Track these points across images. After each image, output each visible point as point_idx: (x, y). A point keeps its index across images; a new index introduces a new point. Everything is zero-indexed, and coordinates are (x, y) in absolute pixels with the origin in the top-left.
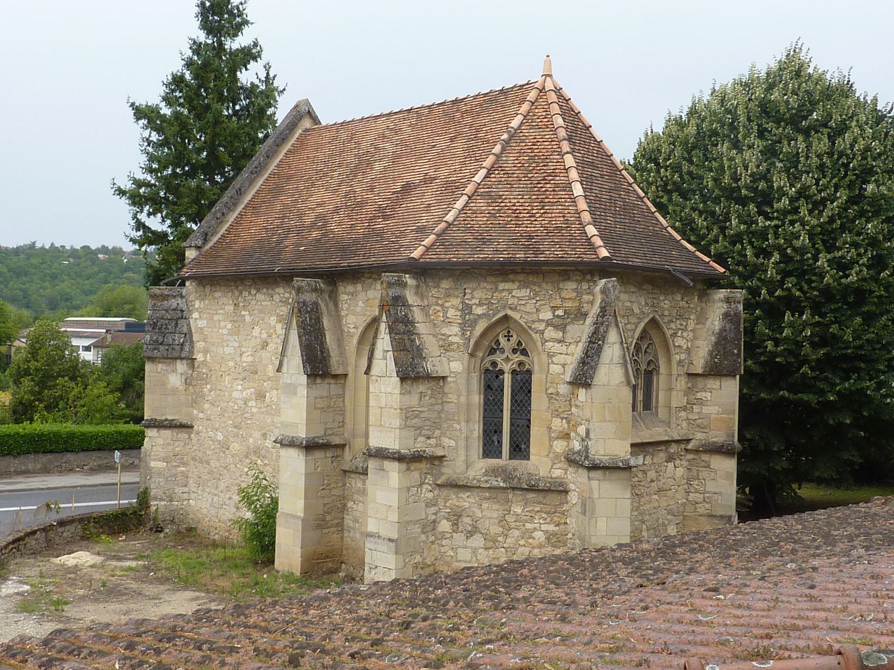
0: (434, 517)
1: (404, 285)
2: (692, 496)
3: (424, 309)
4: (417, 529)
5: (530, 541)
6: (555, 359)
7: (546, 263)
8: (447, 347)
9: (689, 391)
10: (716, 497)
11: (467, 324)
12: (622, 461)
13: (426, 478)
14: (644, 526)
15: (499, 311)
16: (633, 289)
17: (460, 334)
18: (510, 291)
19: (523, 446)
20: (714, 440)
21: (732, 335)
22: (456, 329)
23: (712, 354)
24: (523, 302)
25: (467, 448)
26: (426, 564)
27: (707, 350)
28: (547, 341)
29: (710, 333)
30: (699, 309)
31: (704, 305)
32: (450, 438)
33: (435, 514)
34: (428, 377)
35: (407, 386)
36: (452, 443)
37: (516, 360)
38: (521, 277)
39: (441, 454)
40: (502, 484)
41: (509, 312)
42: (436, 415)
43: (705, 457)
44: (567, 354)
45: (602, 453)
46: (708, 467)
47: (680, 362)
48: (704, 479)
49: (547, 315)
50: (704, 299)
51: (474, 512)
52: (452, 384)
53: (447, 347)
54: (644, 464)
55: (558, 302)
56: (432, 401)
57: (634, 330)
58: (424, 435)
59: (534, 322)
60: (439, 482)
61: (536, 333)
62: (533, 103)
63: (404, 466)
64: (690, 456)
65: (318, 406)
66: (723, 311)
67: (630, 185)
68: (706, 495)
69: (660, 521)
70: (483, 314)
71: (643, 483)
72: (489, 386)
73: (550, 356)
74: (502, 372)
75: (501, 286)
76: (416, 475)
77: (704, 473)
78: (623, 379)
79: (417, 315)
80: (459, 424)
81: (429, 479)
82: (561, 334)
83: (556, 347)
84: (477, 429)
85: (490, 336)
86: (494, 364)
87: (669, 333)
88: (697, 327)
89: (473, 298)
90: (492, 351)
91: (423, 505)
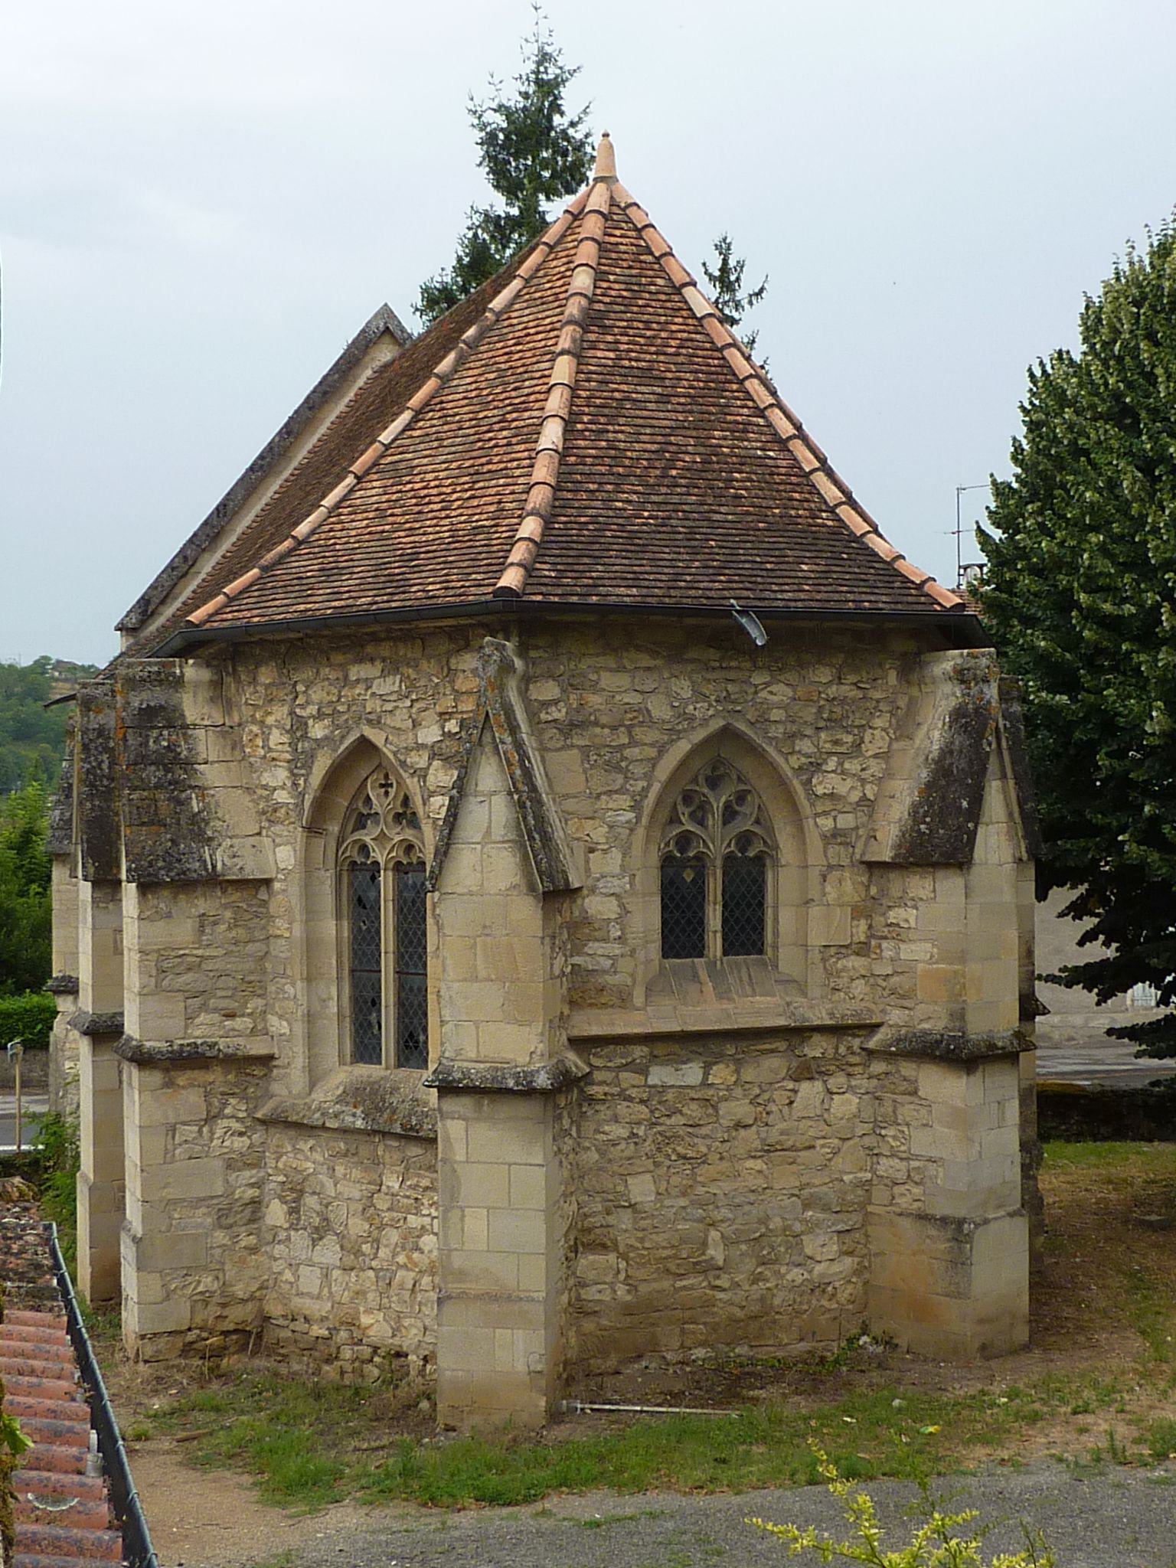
0: (251, 1192)
1: (179, 682)
2: (886, 1166)
3: (228, 733)
4: (203, 1218)
5: (416, 1255)
7: (420, 613)
8: (270, 814)
10: (932, 1167)
11: (300, 763)
12: (517, 1076)
13: (225, 1105)
14: (714, 1235)
15: (349, 730)
16: (646, 661)
17: (289, 784)
18: (368, 683)
20: (926, 1026)
21: (963, 765)
22: (282, 775)
23: (916, 812)
24: (389, 707)
25: (312, 1040)
26: (233, 1296)
27: (908, 801)
29: (922, 759)
30: (902, 702)
31: (914, 691)
32: (281, 1017)
33: (257, 1185)
34: (214, 881)
35: (162, 901)
37: (397, 839)
38: (385, 650)
39: (262, 1050)
40: (359, 1124)
41: (370, 733)
42: (250, 965)
43: (908, 1069)
45: (473, 1055)
46: (914, 1093)
47: (835, 836)
48: (908, 1125)
49: (430, 734)
50: (915, 677)
51: (323, 1185)
52: (280, 897)
53: (270, 814)
54: (705, 1084)
55: (447, 703)
56: (240, 933)
57: (654, 762)
58: (215, 1010)
60: (259, 1115)
62: (551, 247)
63: (156, 1077)
64: (878, 1067)
66: (953, 703)
67: (761, 413)
68: (914, 1164)
69: (776, 1223)
70: (326, 738)
71: (704, 1131)
72: (360, 900)
75: (356, 672)
76: (193, 1098)
77: (906, 1112)
78: (517, 879)
79: (206, 745)
80: (293, 985)
81: (235, 1106)
84: (335, 997)
85: (350, 786)
86: (364, 849)
87: (787, 766)
88: (895, 746)
89: (308, 703)
90: (361, 823)
91: (219, 1164)
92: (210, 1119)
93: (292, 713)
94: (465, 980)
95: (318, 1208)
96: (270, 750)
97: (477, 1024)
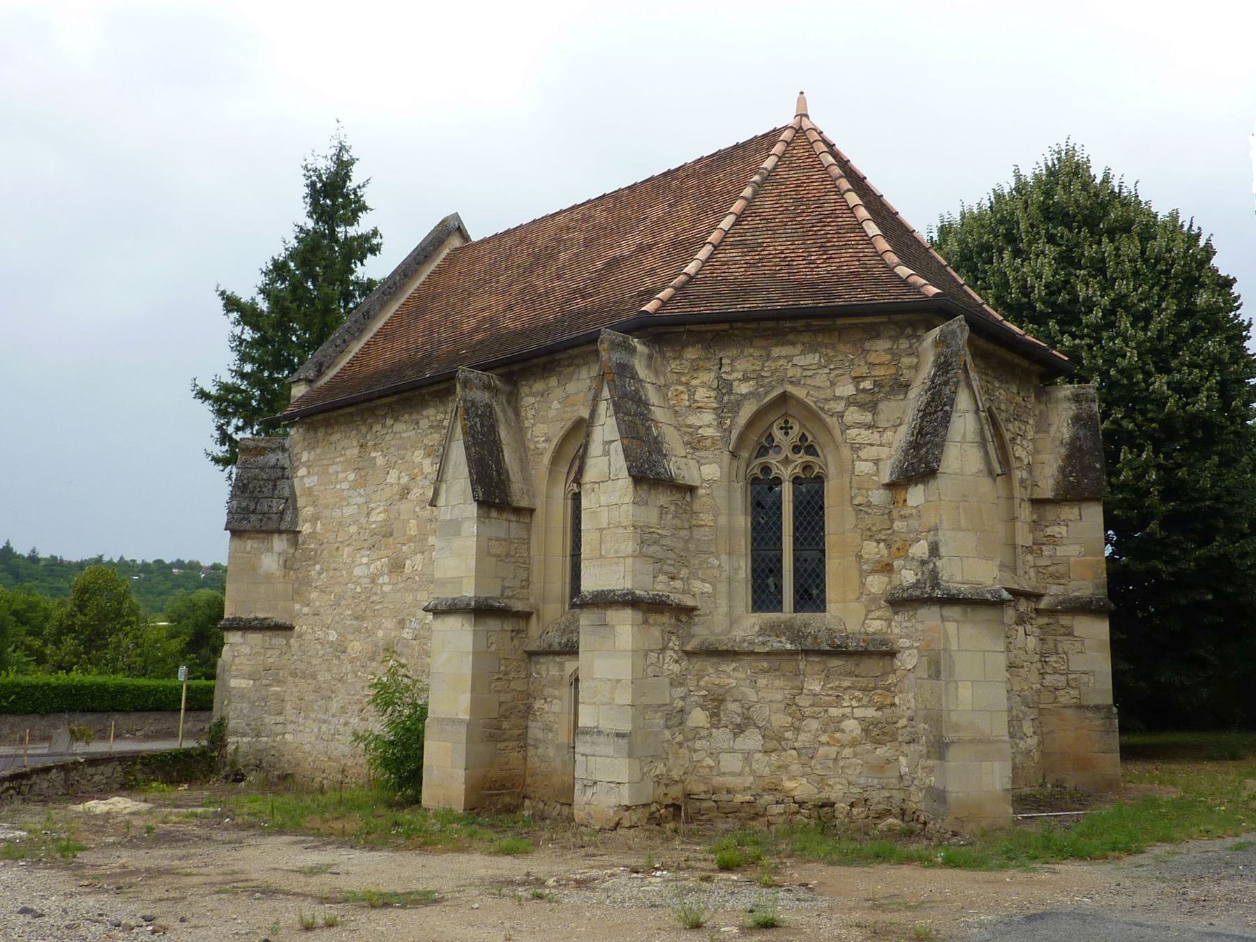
0: (681, 703)
1: (633, 351)
2: (1049, 679)
4: (659, 720)
5: (838, 735)
6: (862, 454)
8: (695, 444)
9: (1036, 525)
10: (1085, 678)
11: (726, 406)
12: (989, 591)
15: (773, 388)
17: (715, 423)
18: (789, 358)
19: (815, 592)
20: (1077, 594)
21: (1089, 444)
22: (708, 417)
24: (810, 373)
25: (730, 595)
26: (671, 779)
27: (1055, 466)
28: (848, 427)
30: (1037, 412)
31: (1043, 407)
32: (703, 581)
33: (683, 698)
35: (643, 492)
36: (708, 588)
37: (800, 461)
38: (806, 338)
40: (789, 646)
41: (790, 389)
43: (1065, 620)
44: (880, 445)
45: (959, 579)
46: (1070, 634)
48: (1066, 653)
49: (847, 390)
51: (744, 694)
53: (695, 444)
55: (864, 370)
58: (666, 573)
59: (827, 400)
60: (688, 648)
61: (832, 416)
62: (788, 144)
63: (639, 616)
64: (1043, 621)
65: (493, 551)
68: (1071, 676)
70: (750, 393)
73: (856, 448)
74: (778, 481)
75: (776, 351)
76: (656, 632)
77: (1065, 644)
78: (982, 467)
79: (652, 396)
81: (674, 643)
82: (870, 416)
83: (864, 435)
84: (743, 569)
86: (766, 469)
87: (1008, 436)
89: (733, 371)
90: (763, 451)
91: (667, 681)
92: (664, 649)
93: (719, 378)
94: (953, 529)
95: (739, 711)
96: (696, 401)
97: (961, 558)
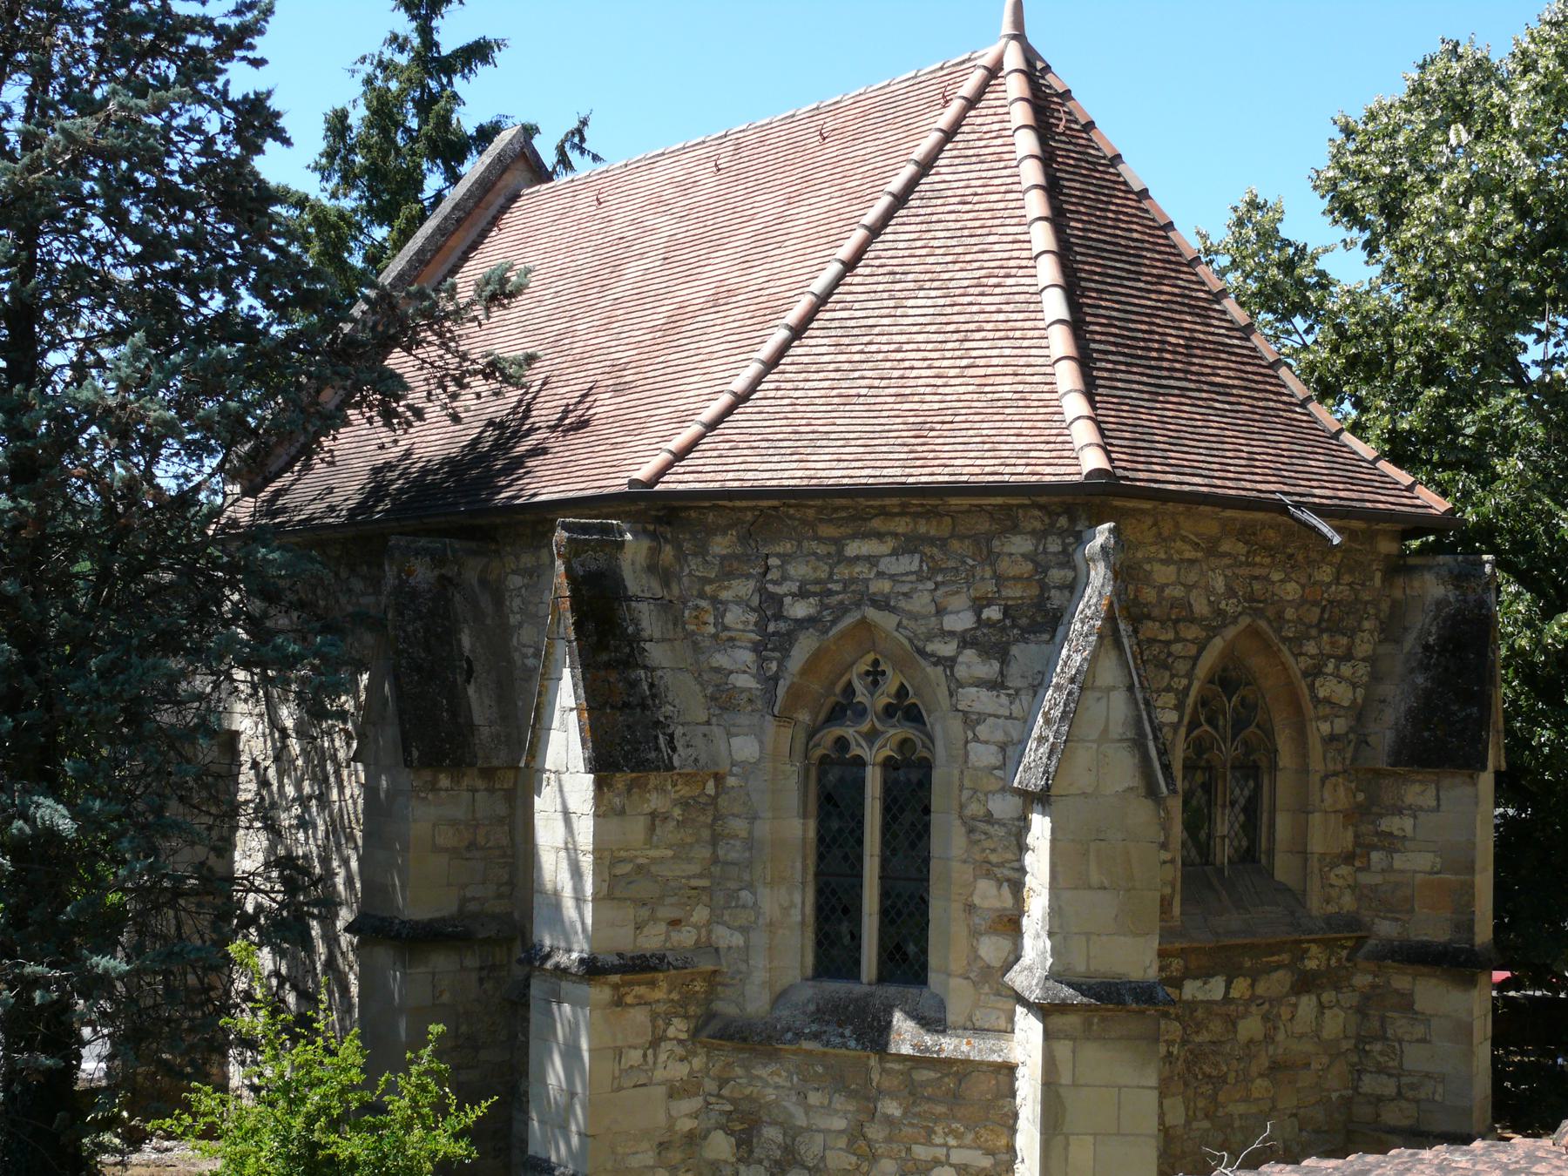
6: (982, 730)
9: (1361, 814)
11: (773, 641)
19: (911, 949)
24: (905, 589)
27: (1403, 708)
28: (961, 686)
36: (738, 940)
44: (1010, 717)
49: (961, 621)
53: (723, 700)
54: (1227, 999)
55: (990, 587)
57: (1195, 659)
59: (930, 638)
61: (935, 664)
65: (440, 841)
73: (971, 721)
74: (860, 762)
77: (1399, 1025)
82: (996, 665)
83: (982, 700)
86: (842, 744)
88: (1382, 650)
89: (785, 578)
91: (662, 1090)
92: (655, 1043)
93: (761, 590)
94: (1076, 888)
95: (780, 1139)
96: (726, 628)
97: (1088, 934)
